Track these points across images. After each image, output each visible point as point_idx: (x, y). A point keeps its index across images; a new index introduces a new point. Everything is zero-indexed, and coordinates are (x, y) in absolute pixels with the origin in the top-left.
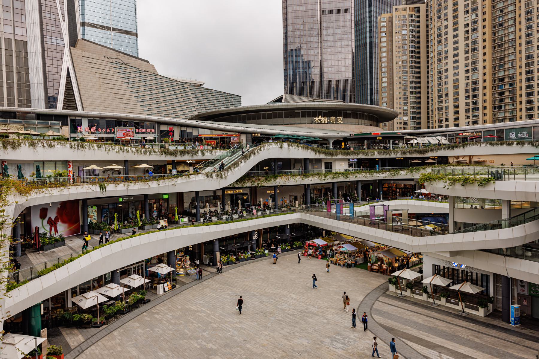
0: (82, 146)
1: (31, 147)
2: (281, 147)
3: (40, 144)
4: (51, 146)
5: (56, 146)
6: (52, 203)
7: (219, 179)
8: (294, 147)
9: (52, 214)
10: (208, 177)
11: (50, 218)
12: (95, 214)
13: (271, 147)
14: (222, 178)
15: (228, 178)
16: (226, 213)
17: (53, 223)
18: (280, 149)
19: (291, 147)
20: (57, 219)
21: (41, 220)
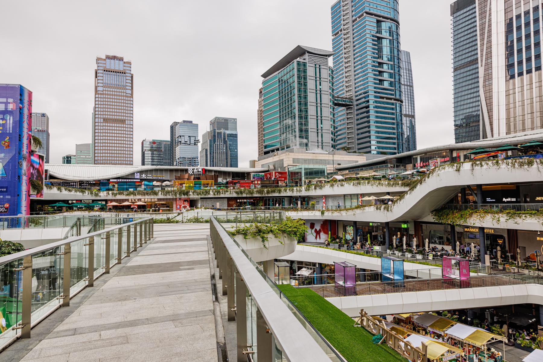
0: (359, 184)
1: (331, 188)
2: (458, 170)
3: (336, 185)
4: (342, 185)
5: (345, 185)
6: (540, 231)
7: (386, 211)
8: (485, 166)
9: (318, 227)
10: (377, 209)
11: (316, 230)
12: (352, 232)
13: (443, 171)
14: (388, 210)
15: (394, 210)
16: (411, 252)
17: (318, 233)
18: (456, 173)
19: (477, 168)
20: (320, 231)
21: (310, 230)
